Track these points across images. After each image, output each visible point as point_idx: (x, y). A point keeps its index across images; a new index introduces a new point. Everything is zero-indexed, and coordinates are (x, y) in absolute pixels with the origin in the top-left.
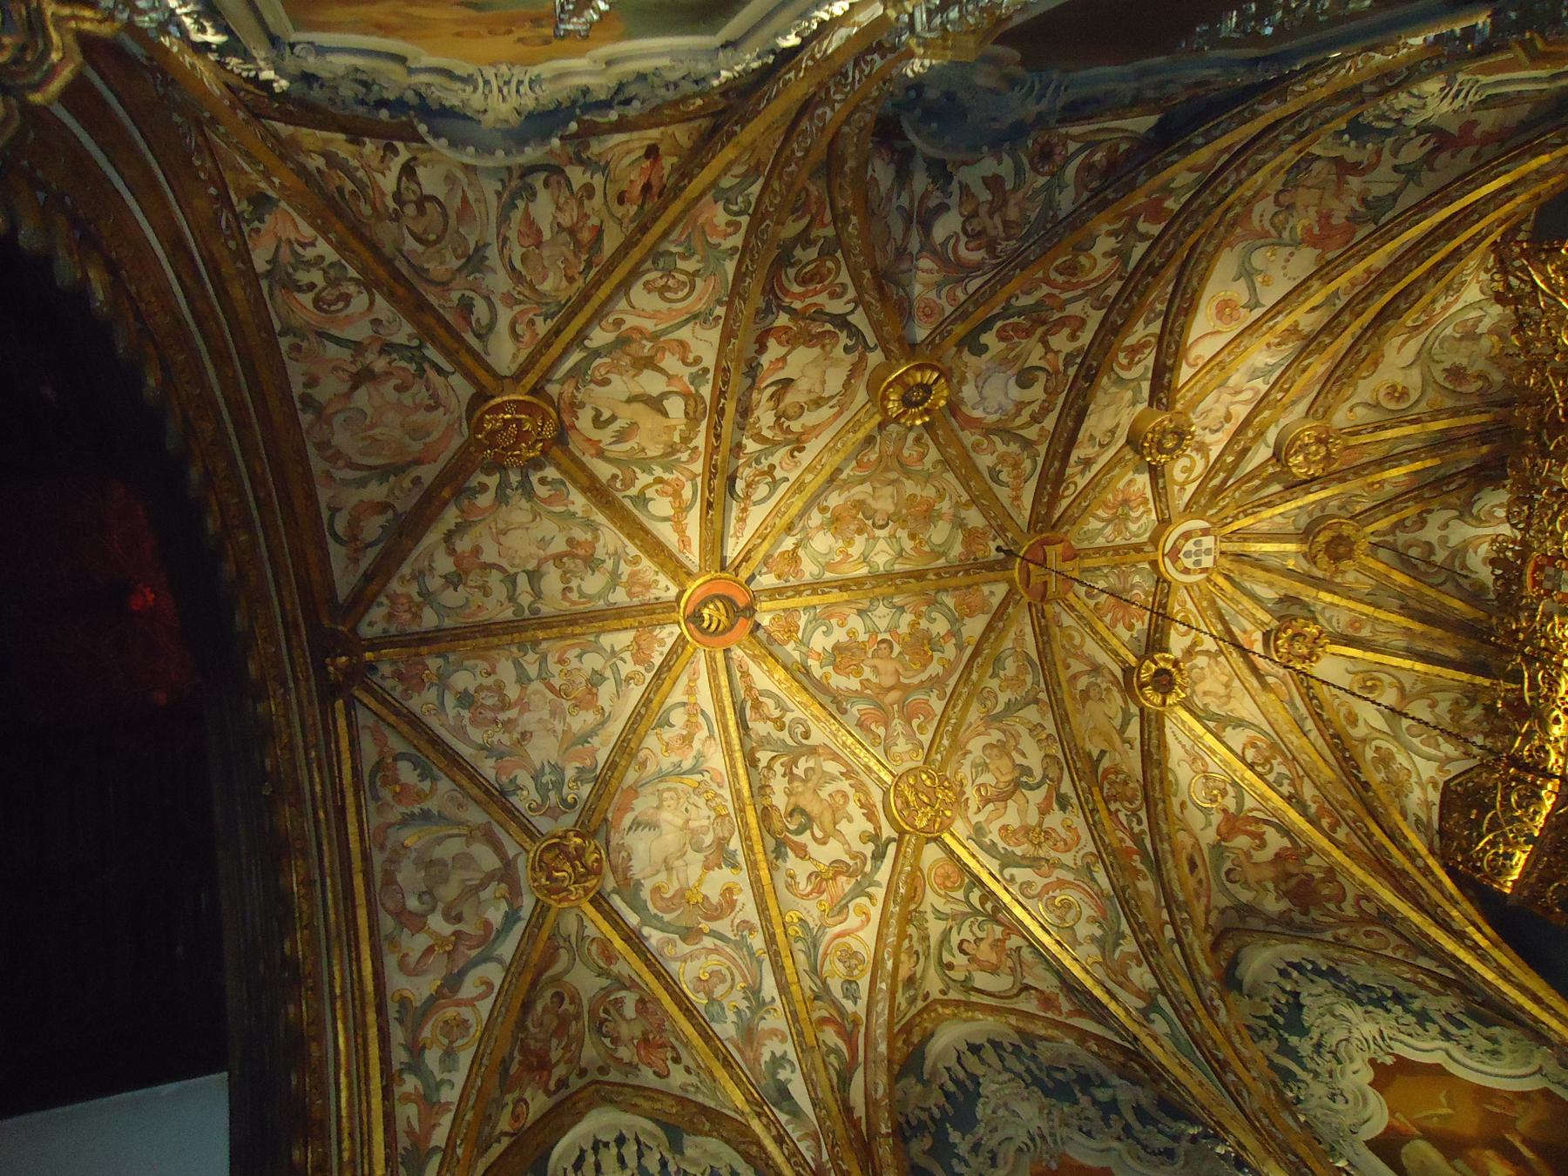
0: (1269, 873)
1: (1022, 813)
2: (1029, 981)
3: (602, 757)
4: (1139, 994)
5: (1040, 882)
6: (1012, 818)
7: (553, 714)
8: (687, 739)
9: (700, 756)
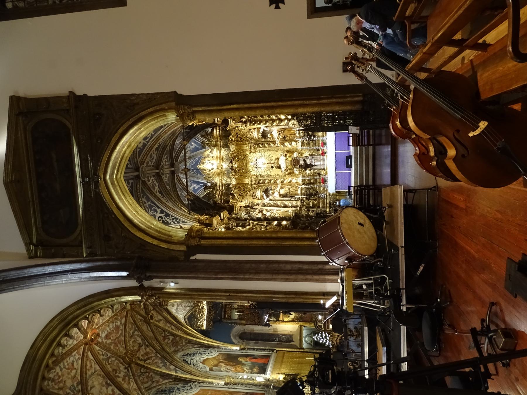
0: (171, 344)
1: (143, 351)
2: (154, 380)
3: (79, 378)
4: (173, 370)
5: (151, 361)
6: (142, 353)
7: (68, 374)
8: (91, 366)
9: (95, 368)
